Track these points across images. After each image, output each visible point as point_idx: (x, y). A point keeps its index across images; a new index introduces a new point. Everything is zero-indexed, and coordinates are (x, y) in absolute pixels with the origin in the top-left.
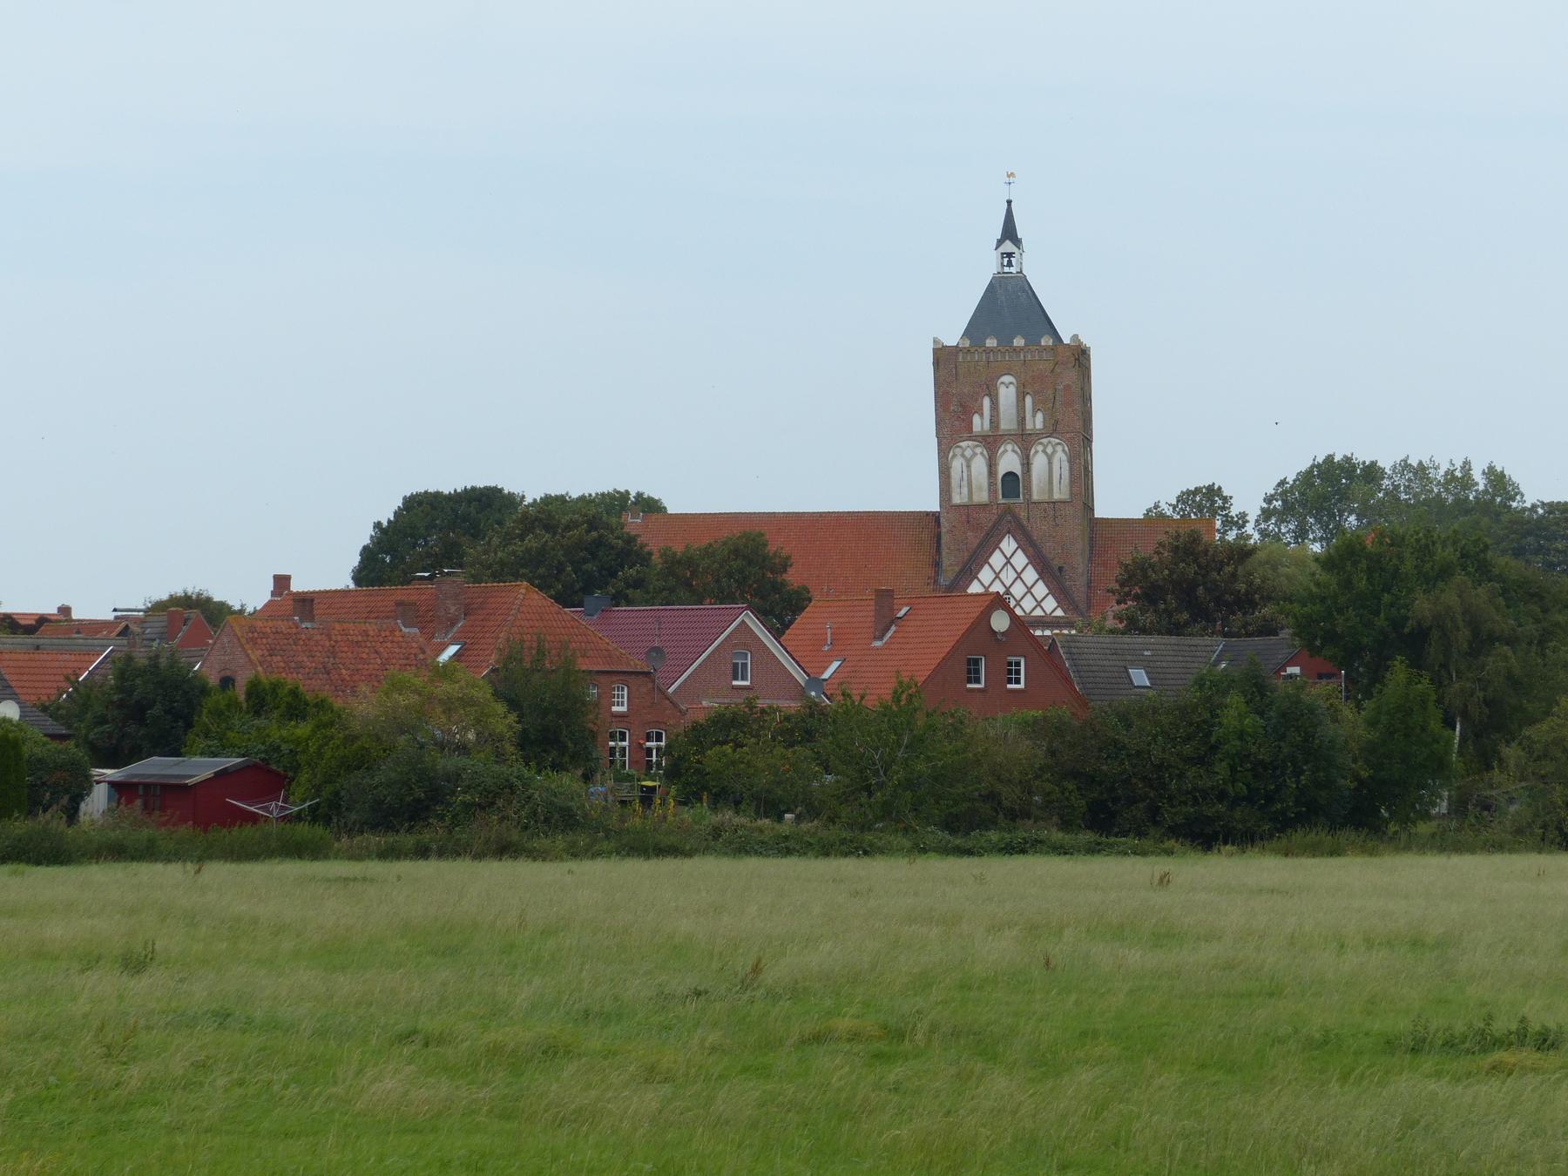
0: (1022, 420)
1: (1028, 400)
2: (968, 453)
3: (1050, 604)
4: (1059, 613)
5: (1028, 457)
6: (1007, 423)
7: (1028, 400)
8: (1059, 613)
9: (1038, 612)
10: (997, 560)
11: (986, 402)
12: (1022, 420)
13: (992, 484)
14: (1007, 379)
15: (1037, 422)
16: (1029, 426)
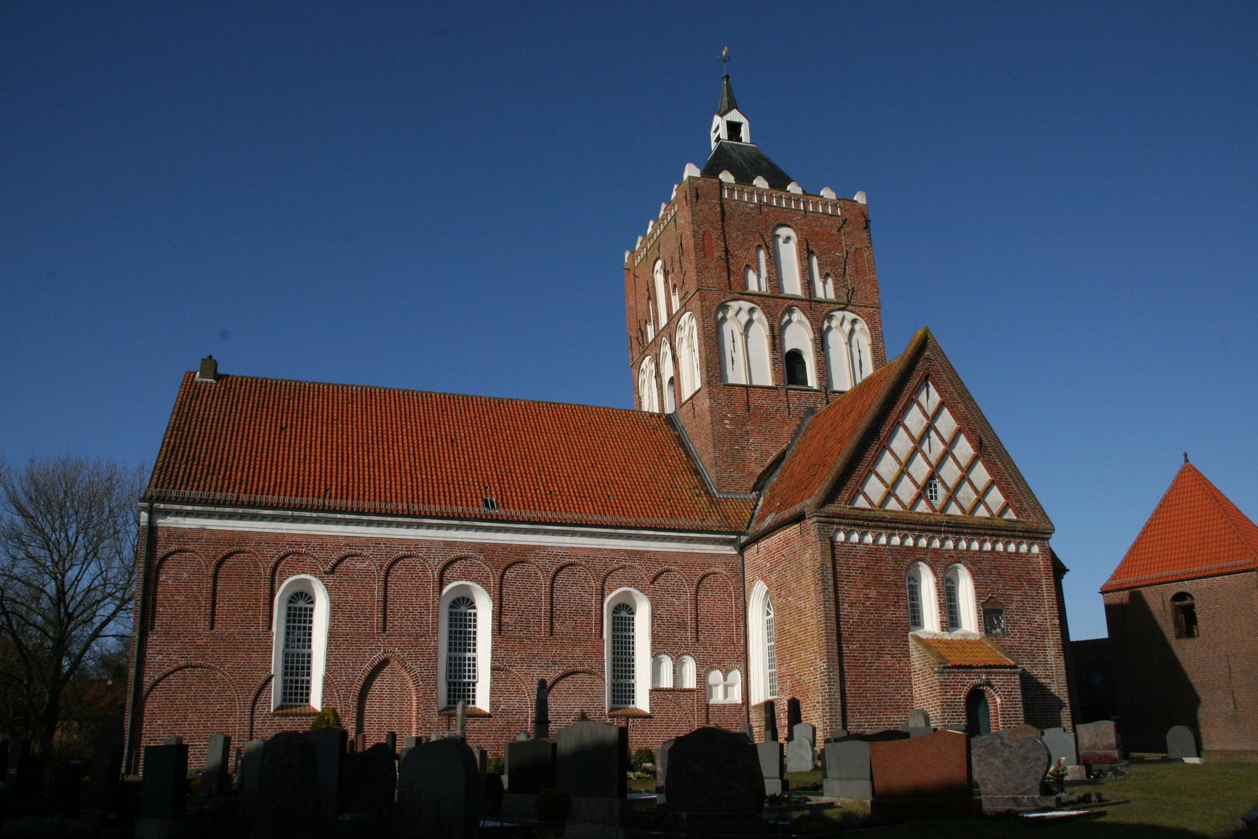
0: (809, 284)
1: (815, 260)
2: (744, 317)
3: (996, 498)
4: (1010, 515)
5: (821, 329)
6: (793, 285)
7: (815, 260)
8: (1010, 515)
9: (982, 512)
10: (914, 420)
11: (762, 255)
12: (809, 284)
13: (774, 362)
14: (783, 232)
15: (825, 290)
16: (820, 294)
